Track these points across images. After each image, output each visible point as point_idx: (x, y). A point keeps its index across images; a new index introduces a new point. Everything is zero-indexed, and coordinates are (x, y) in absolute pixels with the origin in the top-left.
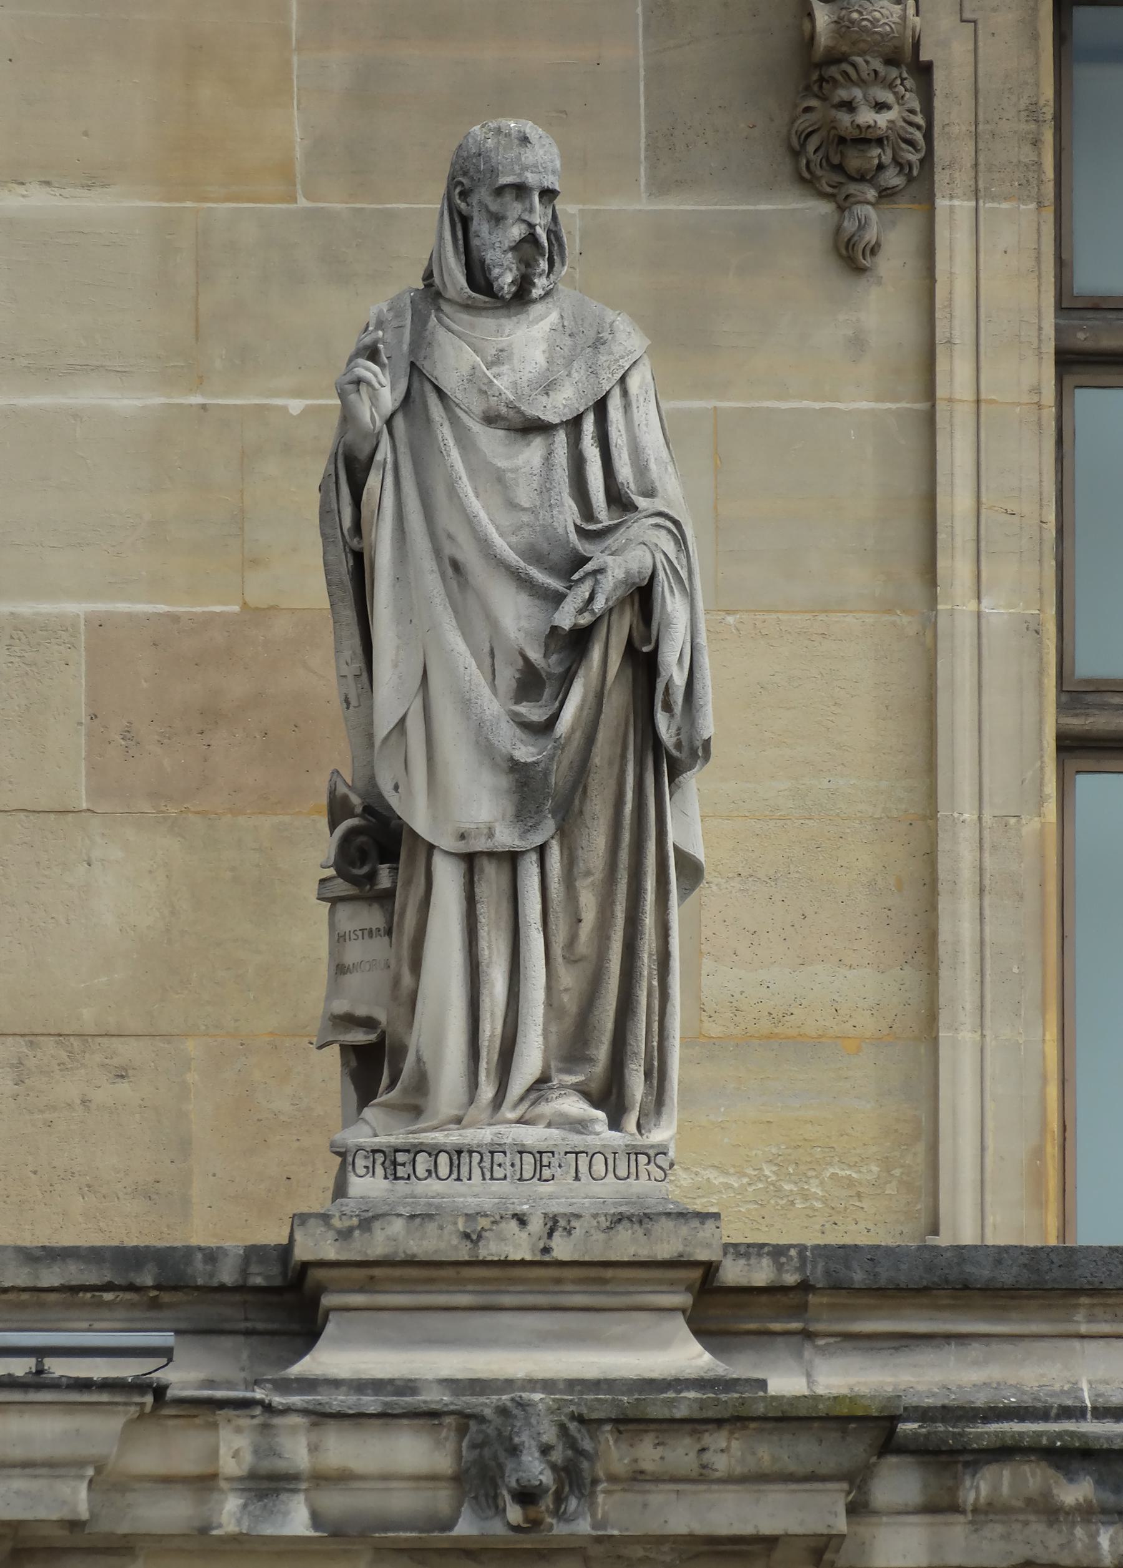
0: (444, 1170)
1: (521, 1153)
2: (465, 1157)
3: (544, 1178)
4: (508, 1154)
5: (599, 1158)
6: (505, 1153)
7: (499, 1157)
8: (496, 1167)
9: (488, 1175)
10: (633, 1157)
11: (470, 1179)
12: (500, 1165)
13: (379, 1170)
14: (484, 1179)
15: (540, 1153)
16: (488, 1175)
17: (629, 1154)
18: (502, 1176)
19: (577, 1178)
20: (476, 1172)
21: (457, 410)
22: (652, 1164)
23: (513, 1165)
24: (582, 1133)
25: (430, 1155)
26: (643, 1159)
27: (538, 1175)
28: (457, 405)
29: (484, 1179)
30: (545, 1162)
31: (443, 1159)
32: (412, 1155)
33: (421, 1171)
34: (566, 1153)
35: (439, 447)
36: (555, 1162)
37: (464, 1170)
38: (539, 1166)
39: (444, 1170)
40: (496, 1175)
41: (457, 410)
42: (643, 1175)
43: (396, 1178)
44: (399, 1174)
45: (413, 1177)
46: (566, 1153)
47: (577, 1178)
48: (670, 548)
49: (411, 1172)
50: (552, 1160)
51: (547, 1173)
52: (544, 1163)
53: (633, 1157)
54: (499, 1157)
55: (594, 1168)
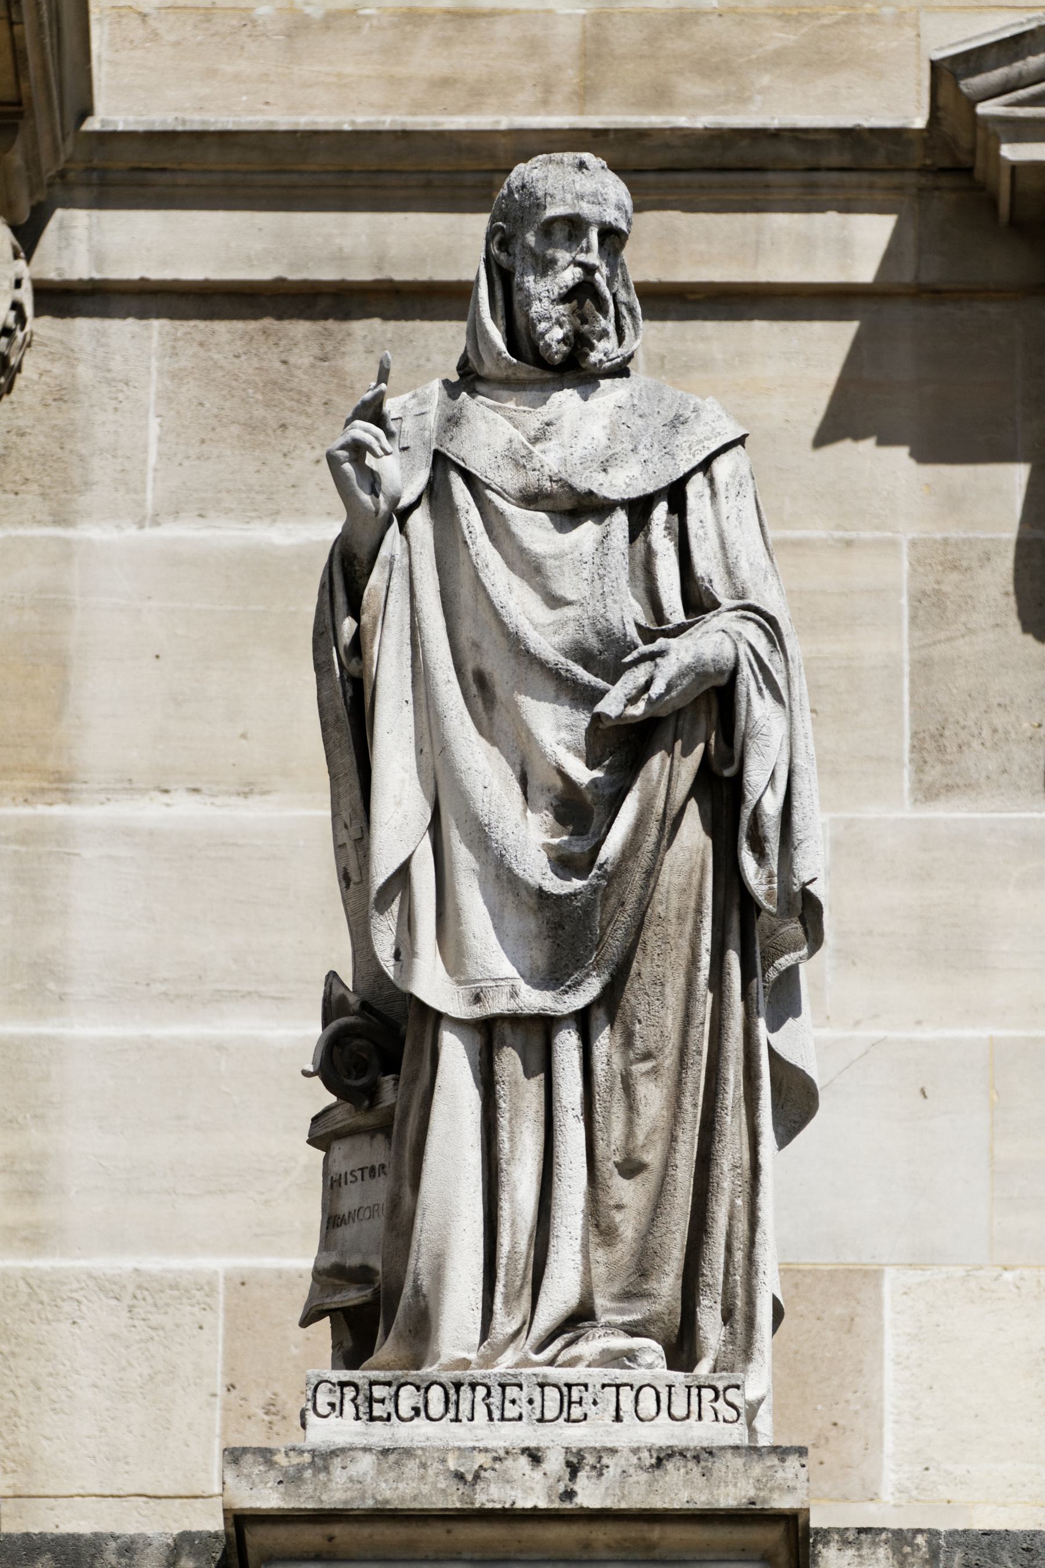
0: (436, 1407)
1: (542, 1386)
2: (465, 1392)
3: (573, 1417)
4: (525, 1387)
5: (648, 1395)
6: (520, 1386)
7: (512, 1392)
8: (507, 1404)
9: (496, 1414)
10: (694, 1391)
11: (472, 1419)
12: (513, 1402)
13: (349, 1408)
14: (491, 1419)
15: (569, 1386)
16: (496, 1414)
17: (689, 1387)
18: (516, 1415)
19: (618, 1418)
20: (481, 1410)
21: (488, 492)
22: (721, 1400)
23: (531, 1402)
24: (629, 1368)
25: (418, 1388)
26: (708, 1394)
27: (565, 1415)
28: (488, 487)
29: (491, 1419)
30: (575, 1397)
31: (436, 1393)
32: (394, 1388)
33: (405, 1410)
34: (604, 1386)
35: (464, 537)
36: (588, 1397)
37: (465, 1407)
38: (566, 1403)
39: (436, 1407)
40: (507, 1415)
41: (488, 492)
42: (708, 1414)
43: (372, 1419)
44: (375, 1413)
45: (394, 1417)
46: (604, 1386)
47: (618, 1418)
48: (762, 646)
49: (392, 1410)
50: (585, 1395)
51: (576, 1412)
52: (573, 1399)
53: (694, 1391)
54: (512, 1392)
55: (641, 1405)
